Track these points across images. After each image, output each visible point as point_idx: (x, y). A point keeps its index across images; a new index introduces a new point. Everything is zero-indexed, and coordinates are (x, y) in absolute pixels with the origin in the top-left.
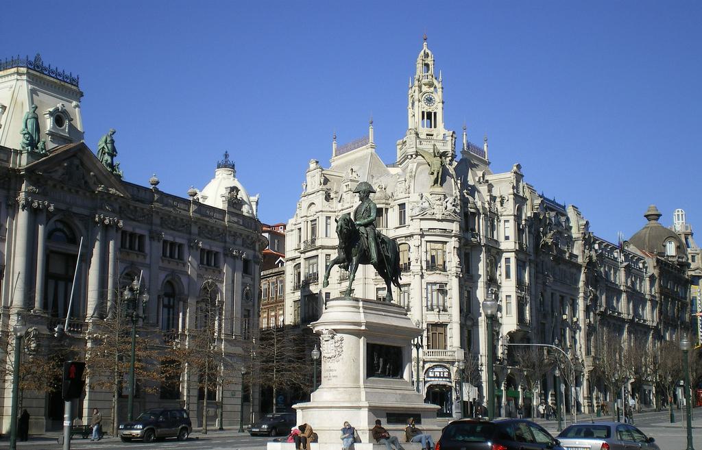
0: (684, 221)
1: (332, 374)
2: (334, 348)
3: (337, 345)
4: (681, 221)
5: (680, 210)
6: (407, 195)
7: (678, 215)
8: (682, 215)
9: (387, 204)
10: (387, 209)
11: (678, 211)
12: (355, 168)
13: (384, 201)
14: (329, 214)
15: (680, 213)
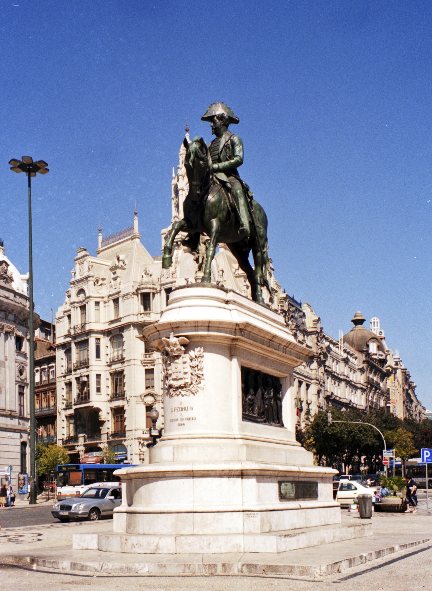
0: (379, 327)
1: (186, 414)
2: (189, 370)
3: (194, 363)
4: (376, 328)
5: (375, 318)
6: (173, 280)
7: (374, 322)
8: (377, 322)
9: (154, 289)
10: (154, 294)
11: (374, 319)
12: (121, 258)
13: (152, 286)
14: (97, 300)
15: (376, 321)
